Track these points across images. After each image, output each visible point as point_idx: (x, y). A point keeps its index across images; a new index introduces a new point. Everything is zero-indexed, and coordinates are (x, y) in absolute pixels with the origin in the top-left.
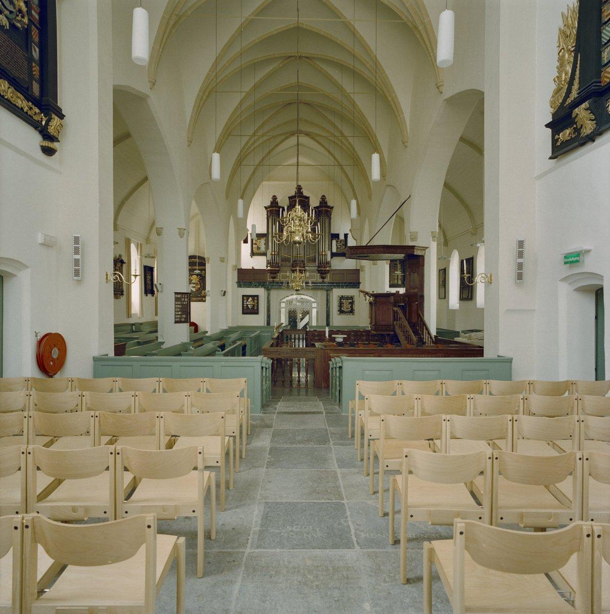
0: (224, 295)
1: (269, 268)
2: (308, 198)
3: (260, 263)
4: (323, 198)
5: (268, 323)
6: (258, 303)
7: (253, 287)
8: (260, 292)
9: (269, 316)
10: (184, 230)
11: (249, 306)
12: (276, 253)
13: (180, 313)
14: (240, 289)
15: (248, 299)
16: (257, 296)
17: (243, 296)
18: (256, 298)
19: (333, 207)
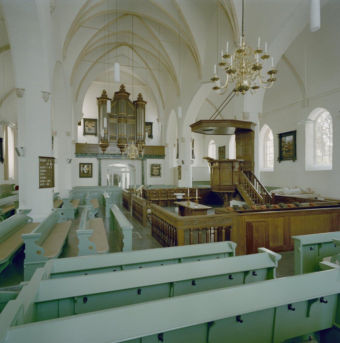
0: (70, 162)
1: (100, 143)
2: (129, 94)
3: (93, 140)
4: (140, 95)
5: (100, 184)
6: (92, 169)
9: (100, 179)
10: (49, 94)
11: (85, 171)
12: (106, 132)
13: (45, 178)
14: (77, 158)
15: (84, 167)
16: (91, 164)
17: (80, 164)
18: (90, 165)
19: (146, 102)
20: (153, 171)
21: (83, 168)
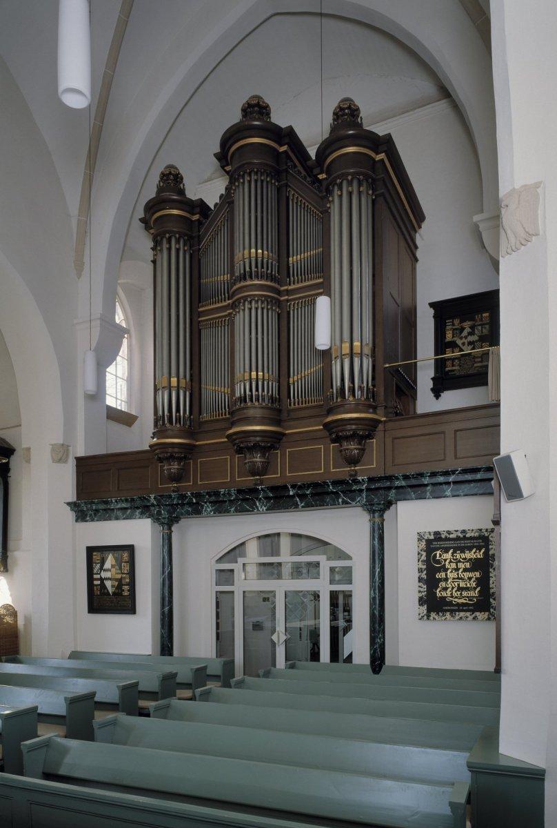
5: (166, 647)
7: (117, 518)
8: (138, 532)
11: (108, 584)
16: (130, 549)
17: (90, 551)
18: (126, 555)
20: (440, 580)
21: (101, 568)
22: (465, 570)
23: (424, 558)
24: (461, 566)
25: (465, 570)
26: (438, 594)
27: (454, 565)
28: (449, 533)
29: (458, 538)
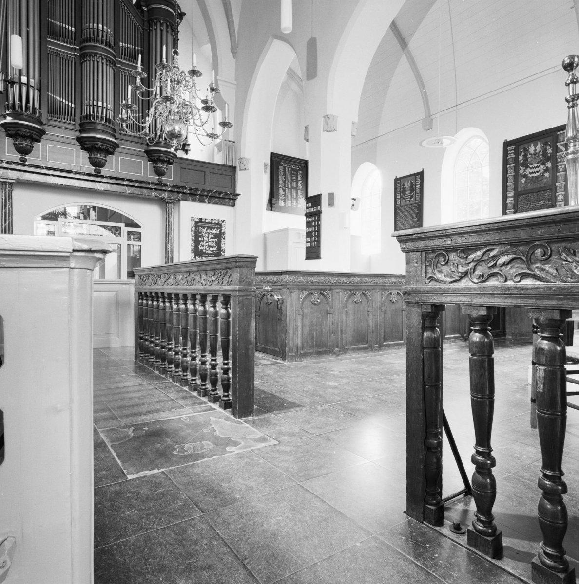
12: (32, 82)
20: (201, 241)
22: (212, 238)
23: (194, 230)
24: (210, 236)
25: (212, 238)
26: (200, 248)
27: (207, 235)
28: (206, 219)
29: (209, 223)
